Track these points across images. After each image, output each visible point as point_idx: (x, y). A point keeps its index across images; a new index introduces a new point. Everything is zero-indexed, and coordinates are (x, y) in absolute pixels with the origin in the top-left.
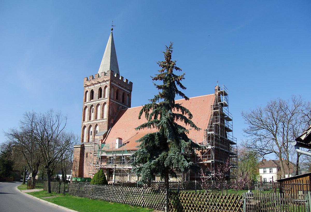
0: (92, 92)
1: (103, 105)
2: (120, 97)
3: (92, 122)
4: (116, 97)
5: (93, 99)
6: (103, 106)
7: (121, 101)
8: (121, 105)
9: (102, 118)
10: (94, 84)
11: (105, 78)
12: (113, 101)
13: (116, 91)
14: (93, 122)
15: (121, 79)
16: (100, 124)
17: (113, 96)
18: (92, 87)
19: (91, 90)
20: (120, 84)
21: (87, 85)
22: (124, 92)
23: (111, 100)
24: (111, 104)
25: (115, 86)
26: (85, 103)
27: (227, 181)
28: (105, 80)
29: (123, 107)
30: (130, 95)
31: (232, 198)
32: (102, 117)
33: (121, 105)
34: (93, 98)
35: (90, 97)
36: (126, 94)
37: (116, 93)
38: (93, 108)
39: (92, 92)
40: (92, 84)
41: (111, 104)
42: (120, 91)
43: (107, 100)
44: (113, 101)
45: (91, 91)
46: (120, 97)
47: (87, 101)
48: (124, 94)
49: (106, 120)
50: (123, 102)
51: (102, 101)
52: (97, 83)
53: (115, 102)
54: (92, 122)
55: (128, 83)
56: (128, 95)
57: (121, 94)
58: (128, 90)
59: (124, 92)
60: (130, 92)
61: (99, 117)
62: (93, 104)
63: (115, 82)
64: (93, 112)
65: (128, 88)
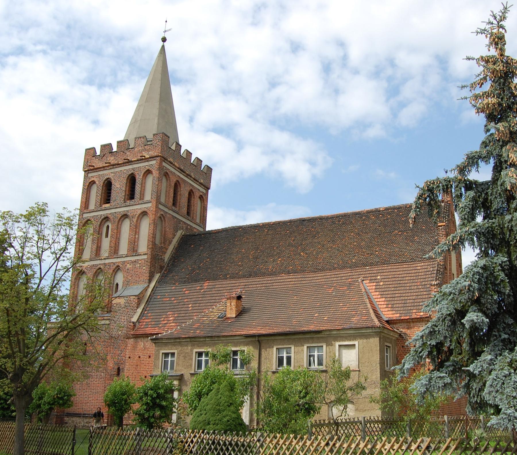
0: (108, 185)
1: (138, 218)
2: (183, 200)
3: (103, 262)
4: (174, 200)
5: (109, 203)
6: (137, 221)
7: (185, 210)
8: (184, 220)
9: (134, 251)
10: (114, 166)
11: (145, 150)
12: (166, 210)
13: (173, 185)
14: (107, 261)
15: (174, 149)
16: (128, 266)
17: (166, 196)
18: (108, 173)
19: (104, 179)
20: (182, 168)
21: (92, 168)
22: (191, 190)
23: (161, 207)
24: (160, 217)
25: (171, 172)
26: (86, 211)
27: (448, 418)
28: (147, 156)
29: (189, 227)
30: (203, 199)
31: (455, 446)
32: (133, 249)
33: (184, 220)
34: (109, 200)
35: (99, 198)
36: (197, 194)
37: (172, 190)
38: (108, 227)
39: (108, 185)
40: (107, 165)
41: (160, 217)
42: (182, 185)
43: (150, 205)
44: (166, 210)
45: (104, 183)
46: (183, 200)
47: (92, 207)
48: (191, 193)
49: (145, 257)
50: (188, 213)
51: (135, 208)
52: (121, 164)
53: (171, 212)
54: (103, 262)
55: (192, 162)
56: (201, 197)
57: (184, 192)
58: (201, 184)
59: (191, 190)
60: (204, 191)
61: (124, 249)
62: (109, 216)
63: (171, 163)
64: (107, 236)
65: (202, 181)
